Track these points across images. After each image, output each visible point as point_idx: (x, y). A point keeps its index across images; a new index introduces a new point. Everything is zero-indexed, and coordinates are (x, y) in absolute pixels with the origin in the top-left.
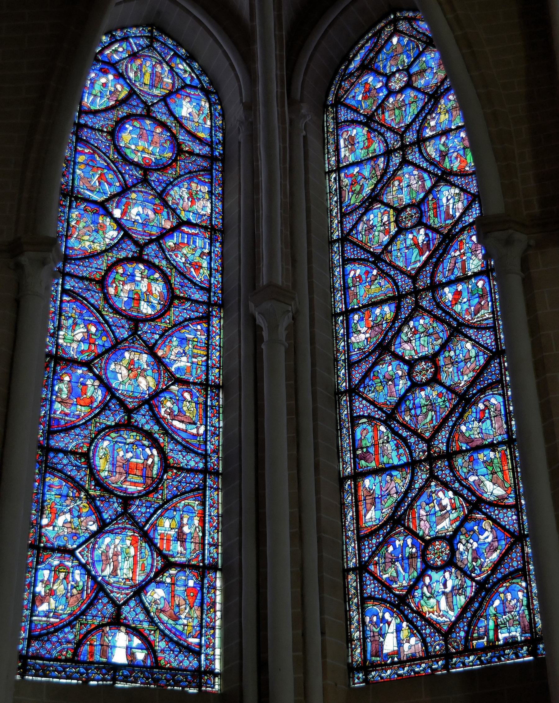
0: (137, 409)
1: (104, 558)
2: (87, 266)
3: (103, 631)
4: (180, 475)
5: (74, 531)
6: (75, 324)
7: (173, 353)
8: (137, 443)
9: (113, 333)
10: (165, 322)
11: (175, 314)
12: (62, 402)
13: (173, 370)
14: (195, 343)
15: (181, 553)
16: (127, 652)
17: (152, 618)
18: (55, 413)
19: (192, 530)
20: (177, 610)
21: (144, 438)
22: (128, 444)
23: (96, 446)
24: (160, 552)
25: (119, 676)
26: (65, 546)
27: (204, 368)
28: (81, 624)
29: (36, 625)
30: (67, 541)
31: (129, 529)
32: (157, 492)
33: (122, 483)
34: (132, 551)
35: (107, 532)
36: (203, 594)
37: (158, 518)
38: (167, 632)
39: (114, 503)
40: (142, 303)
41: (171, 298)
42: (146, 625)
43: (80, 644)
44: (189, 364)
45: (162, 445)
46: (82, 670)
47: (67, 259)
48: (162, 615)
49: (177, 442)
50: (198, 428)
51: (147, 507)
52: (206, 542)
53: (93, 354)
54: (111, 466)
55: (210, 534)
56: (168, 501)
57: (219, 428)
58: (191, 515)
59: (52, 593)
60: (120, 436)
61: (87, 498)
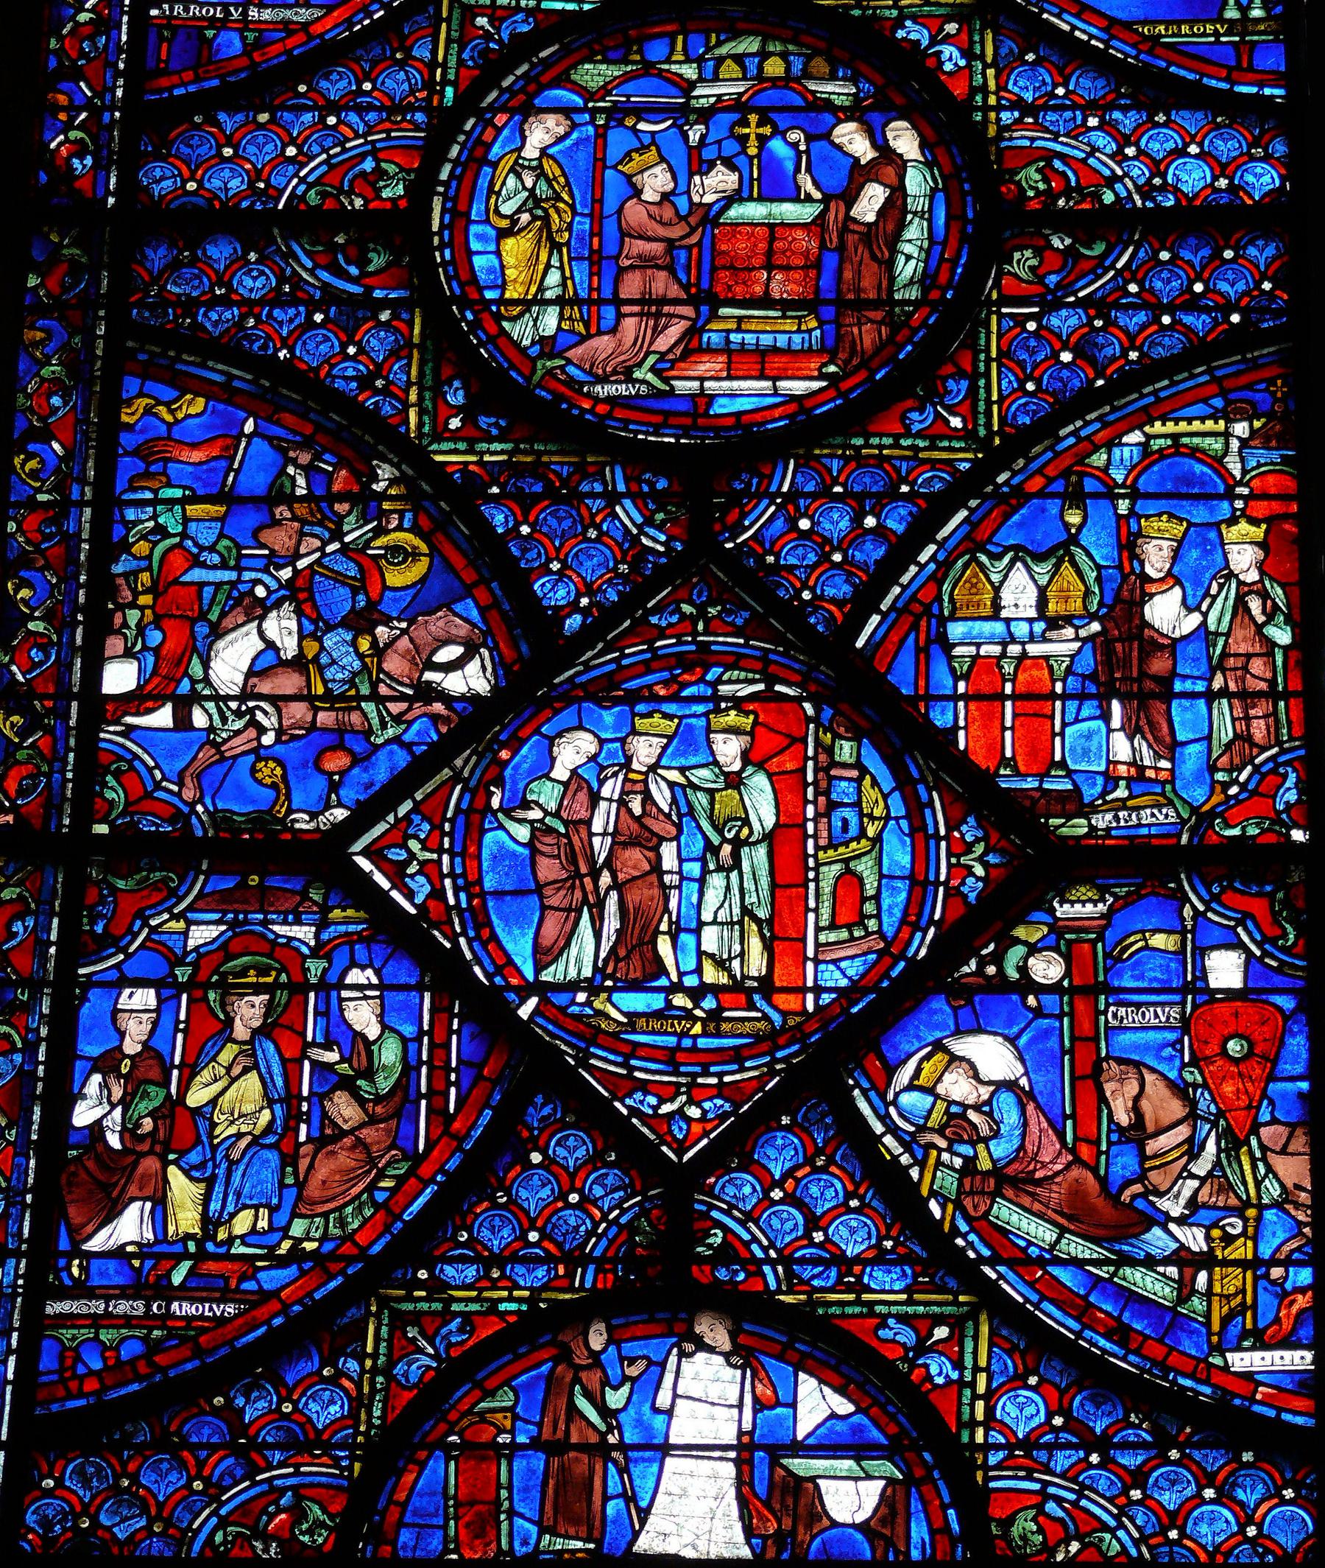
1: (549, 869)
3: (564, 1355)
4: (1099, 266)
5: (325, 718)
8: (771, 97)
15: (1138, 775)
19: (1219, 615)
20: (1124, 1163)
21: (820, 65)
22: (705, 115)
23: (478, 157)
24: (974, 789)
26: (262, 820)
28: (400, 1322)
29: (69, 1356)
30: (282, 788)
31: (733, 661)
32: (935, 394)
34: (761, 803)
37: (944, 567)
38: (1052, 1316)
39: (612, 498)
42: (887, 1284)
43: (393, 1449)
48: (1005, 1213)
49: (1070, 54)
51: (858, 503)
54: (580, 273)
56: (1018, 442)
58: (1200, 514)
59: (179, 1132)
60: (648, 69)
61: (413, 498)
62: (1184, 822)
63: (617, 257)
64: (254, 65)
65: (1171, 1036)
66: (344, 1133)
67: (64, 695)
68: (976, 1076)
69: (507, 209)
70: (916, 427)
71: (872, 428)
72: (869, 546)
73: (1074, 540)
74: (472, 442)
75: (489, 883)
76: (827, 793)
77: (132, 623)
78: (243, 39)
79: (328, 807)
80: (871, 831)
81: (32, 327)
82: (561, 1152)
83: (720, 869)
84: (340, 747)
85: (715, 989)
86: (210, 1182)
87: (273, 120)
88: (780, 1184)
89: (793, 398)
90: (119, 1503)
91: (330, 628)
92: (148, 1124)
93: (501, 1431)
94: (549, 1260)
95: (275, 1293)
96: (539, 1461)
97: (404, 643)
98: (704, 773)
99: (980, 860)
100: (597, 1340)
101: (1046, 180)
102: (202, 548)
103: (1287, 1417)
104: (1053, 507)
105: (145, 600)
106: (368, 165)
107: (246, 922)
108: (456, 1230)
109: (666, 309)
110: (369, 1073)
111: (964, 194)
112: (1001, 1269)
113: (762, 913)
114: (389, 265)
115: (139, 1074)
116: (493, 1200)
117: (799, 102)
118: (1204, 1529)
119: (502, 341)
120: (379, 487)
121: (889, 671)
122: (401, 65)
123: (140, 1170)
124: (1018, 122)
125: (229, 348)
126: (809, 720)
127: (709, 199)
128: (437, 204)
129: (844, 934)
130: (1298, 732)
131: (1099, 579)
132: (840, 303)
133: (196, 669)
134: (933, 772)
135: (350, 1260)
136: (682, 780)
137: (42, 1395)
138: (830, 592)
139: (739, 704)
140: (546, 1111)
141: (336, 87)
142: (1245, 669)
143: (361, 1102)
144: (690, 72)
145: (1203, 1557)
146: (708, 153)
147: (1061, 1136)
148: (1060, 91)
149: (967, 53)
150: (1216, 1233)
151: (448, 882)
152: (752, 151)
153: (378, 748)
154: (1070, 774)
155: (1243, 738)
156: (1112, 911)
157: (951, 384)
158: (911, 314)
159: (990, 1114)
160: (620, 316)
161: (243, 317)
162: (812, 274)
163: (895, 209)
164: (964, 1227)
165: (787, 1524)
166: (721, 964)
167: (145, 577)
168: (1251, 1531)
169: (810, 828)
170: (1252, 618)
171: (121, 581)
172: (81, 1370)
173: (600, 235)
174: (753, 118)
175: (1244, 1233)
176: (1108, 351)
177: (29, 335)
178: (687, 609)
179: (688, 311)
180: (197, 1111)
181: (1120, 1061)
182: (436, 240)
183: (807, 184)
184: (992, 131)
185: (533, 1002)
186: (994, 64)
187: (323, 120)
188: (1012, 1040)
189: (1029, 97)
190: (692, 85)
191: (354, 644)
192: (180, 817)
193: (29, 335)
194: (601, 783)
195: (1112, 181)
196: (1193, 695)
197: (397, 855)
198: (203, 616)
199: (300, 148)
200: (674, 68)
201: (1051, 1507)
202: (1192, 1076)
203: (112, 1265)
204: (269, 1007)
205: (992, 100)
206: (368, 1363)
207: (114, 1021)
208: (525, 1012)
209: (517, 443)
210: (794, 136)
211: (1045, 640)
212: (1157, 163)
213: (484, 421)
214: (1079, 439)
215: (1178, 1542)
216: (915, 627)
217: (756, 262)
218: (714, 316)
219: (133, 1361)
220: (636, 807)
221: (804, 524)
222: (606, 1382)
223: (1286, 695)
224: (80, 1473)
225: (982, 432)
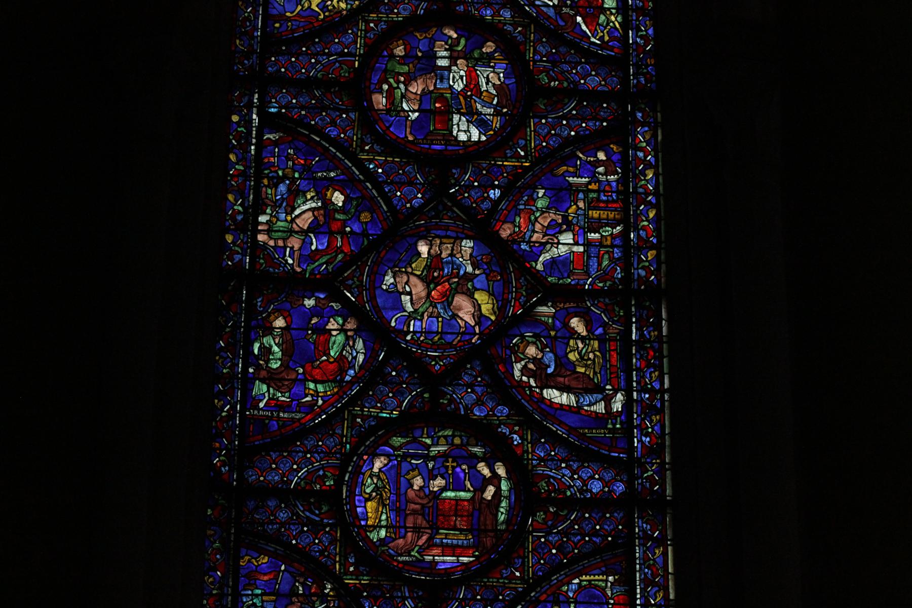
0: (452, 374)
2: (318, 54)
4: (566, 518)
6: (295, 193)
7: (538, 227)
9: (388, 201)
10: (517, 157)
11: (536, 135)
12: (272, 378)
13: (540, 267)
14: (592, 195)
18: (256, 407)
22: (434, 458)
23: (358, 472)
27: (617, 253)
32: (510, 564)
33: (422, 551)
39: (404, 598)
40: (456, 118)
41: (524, 98)
44: (581, 249)
47: (273, 43)
50: (608, 400)
53: (340, 257)
56: (538, 581)
57: (662, 391)
61: (337, 596)
69: (368, 491)
78: (278, 424)
81: (210, 529)
89: (463, 564)
101: (548, 486)
106: (321, 473)
117: (465, 454)
122: (332, 436)
124: (539, 464)
127: (436, 489)
141: (309, 443)
146: (435, 472)
152: (450, 472)
160: (406, 532)
161: (280, 528)
163: (498, 494)
174: (450, 460)
177: (209, 532)
179: (429, 531)
184: (530, 467)
186: (531, 443)
189: (542, 454)
190: (430, 446)
193: (209, 532)
195: (570, 487)
205: (530, 456)
210: (464, 467)
213: (361, 568)
214: (558, 581)
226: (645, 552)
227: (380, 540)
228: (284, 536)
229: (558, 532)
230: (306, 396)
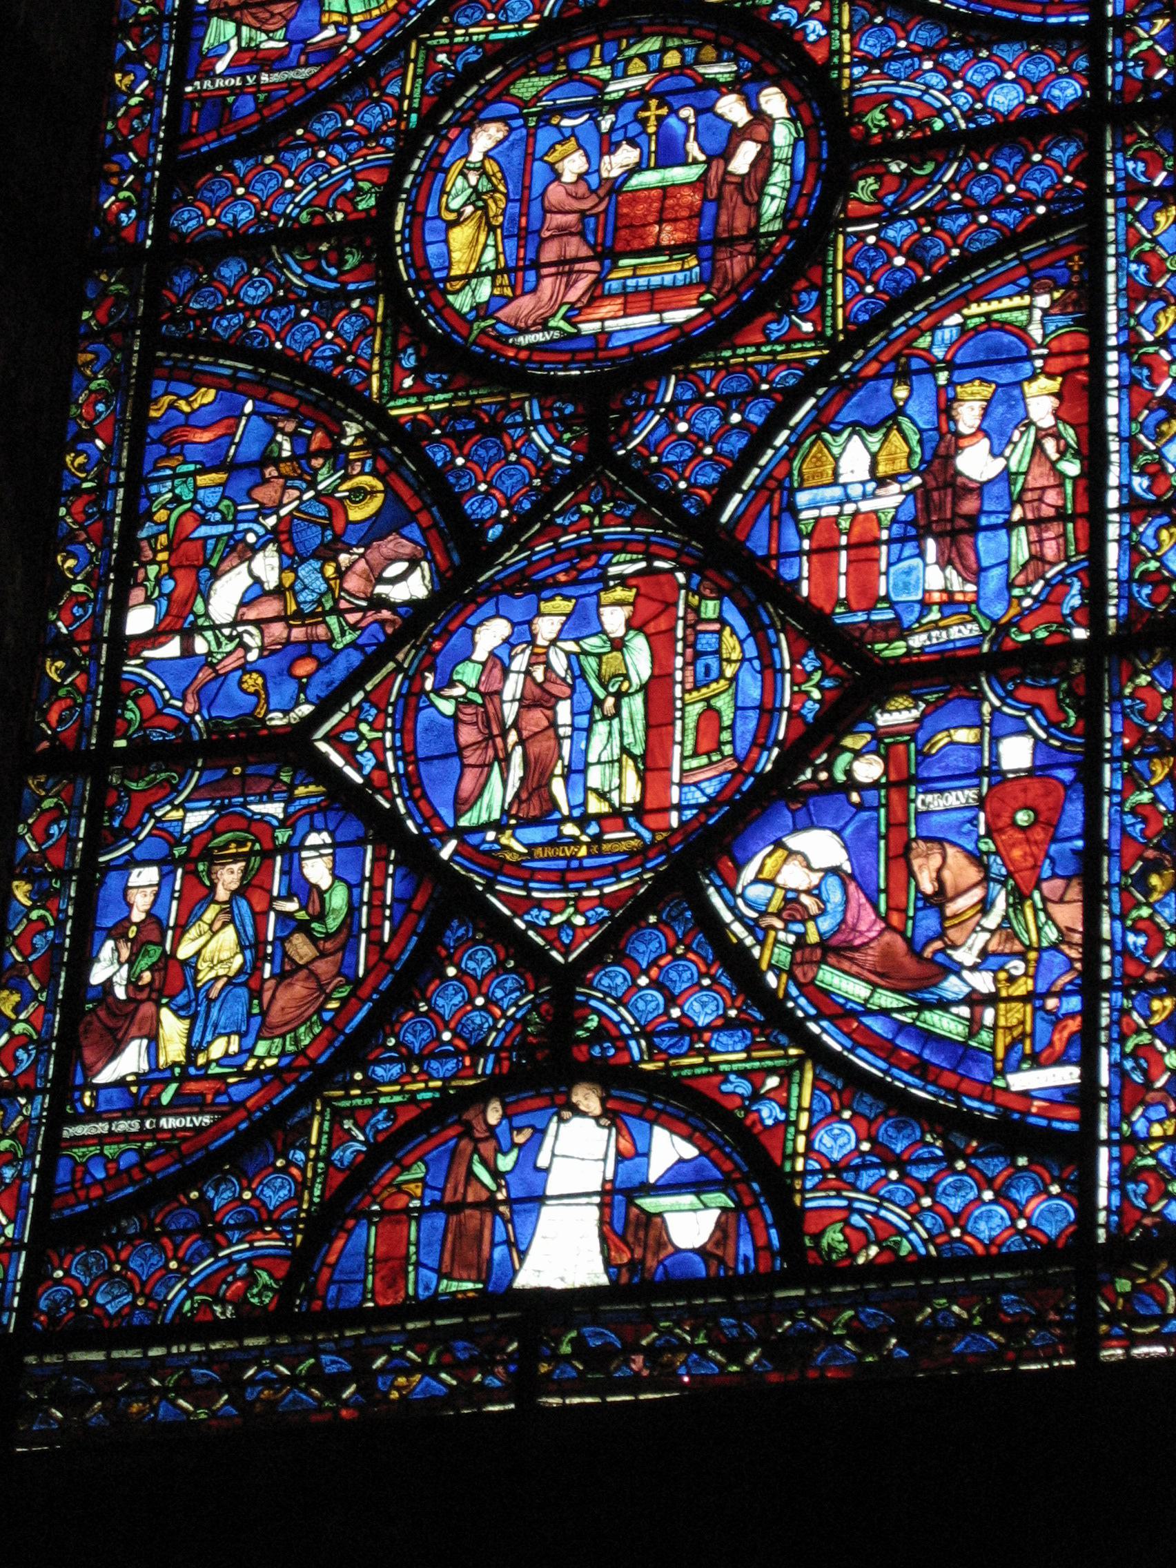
4: (930, 181)
8: (670, 83)
16: (605, 1223)
17: (772, 1004)
18: (211, 75)
19: (1018, 457)
21: (709, 52)
22: (615, 106)
24: (816, 629)
25: (556, 1358)
28: (338, 1115)
31: (623, 546)
32: (790, 307)
35: (492, 591)
36: (1093, 793)
39: (529, 425)
43: (327, 1221)
45: (820, 55)
46: (333, 1364)
48: (829, 977)
52: (1113, 499)
55: (1133, 448)
56: (858, 335)
58: (1006, 376)
59: (172, 981)
60: (572, 76)
62: (984, 633)
63: (539, 231)
64: (263, 118)
65: (969, 814)
66: (300, 967)
67: (96, 640)
68: (809, 867)
69: (455, 204)
70: (774, 336)
71: (738, 341)
72: (734, 438)
73: (901, 411)
74: (420, 396)
75: (422, 753)
76: (693, 645)
77: (152, 576)
79: (297, 704)
80: (729, 671)
81: (85, 351)
82: (472, 964)
83: (605, 718)
84: (309, 655)
85: (599, 817)
86: (193, 1018)
87: (276, 161)
88: (646, 972)
89: (676, 326)
90: (112, 1285)
91: (303, 560)
92: (147, 977)
93: (412, 1197)
94: (458, 1053)
95: (242, 1104)
96: (439, 1220)
97: (362, 565)
98: (595, 641)
99: (818, 685)
100: (494, 1116)
101: (887, 118)
102: (207, 510)
103: (1056, 1125)
104: (884, 385)
105: (162, 556)
106: (349, 185)
107: (231, 805)
108: (386, 1037)
109: (577, 267)
110: (321, 917)
111: (821, 139)
112: (825, 1024)
113: (638, 750)
114: (361, 262)
115: (142, 937)
116: (416, 1009)
117: (690, 83)
118: (982, 1226)
119: (447, 312)
120: (346, 442)
121: (748, 538)
122: (377, 102)
123: (139, 1015)
124: (867, 74)
125: (235, 348)
126: (681, 587)
128: (401, 208)
129: (704, 760)
130: (1083, 547)
131: (920, 442)
132: (718, 242)
133: (199, 606)
134: (782, 618)
135: (302, 1069)
136: (576, 649)
137: (57, 1203)
138: (701, 480)
139: (623, 581)
140: (461, 931)
141: (325, 126)
142: (1040, 500)
143: (314, 940)
144: (604, 73)
145: (980, 1249)
147: (875, 907)
148: (902, 44)
149: (828, 25)
150: (1002, 975)
151: (389, 755)
153: (337, 652)
154: (893, 605)
155: (1037, 558)
156: (924, 714)
157: (804, 297)
158: (772, 244)
159: (818, 896)
160: (539, 278)
161: (247, 320)
162: (695, 221)
163: (764, 161)
164: (794, 992)
165: (638, 1253)
166: (603, 796)
167: (163, 539)
168: (1022, 1224)
169: (678, 676)
170: (1047, 457)
171: (144, 544)
172: (88, 1180)
173: (527, 215)
174: (653, 103)
175: (1026, 974)
176: (935, 252)
178: (586, 508)
179: (594, 266)
180: (185, 963)
181: (927, 839)
182: (398, 238)
183: (693, 149)
184: (845, 84)
185: (452, 844)
186: (849, 30)
187: (314, 153)
188: (838, 832)
190: (606, 83)
191: (322, 571)
192: (183, 726)
193: (84, 357)
194: (511, 658)
195: (940, 112)
196: (992, 528)
197: (350, 737)
198: (206, 563)
199: (296, 179)
200: (593, 72)
201: (856, 1220)
202: (987, 845)
203: (115, 1093)
204: (245, 871)
206: (312, 1153)
207: (125, 896)
208: (445, 854)
209: (455, 391)
210: (687, 112)
211: (874, 496)
212: (979, 90)
213: (430, 378)
214: (909, 328)
215: (959, 1240)
216: (770, 500)
217: (651, 219)
218: (615, 267)
219: (128, 1170)
220: (539, 673)
221: (682, 427)
222: (500, 1150)
223: (1072, 518)
224: (84, 1263)
225: (829, 332)
226: (1129, 225)
227: (476, 307)
228: (252, 337)
229: (914, 215)
230: (323, 27)
